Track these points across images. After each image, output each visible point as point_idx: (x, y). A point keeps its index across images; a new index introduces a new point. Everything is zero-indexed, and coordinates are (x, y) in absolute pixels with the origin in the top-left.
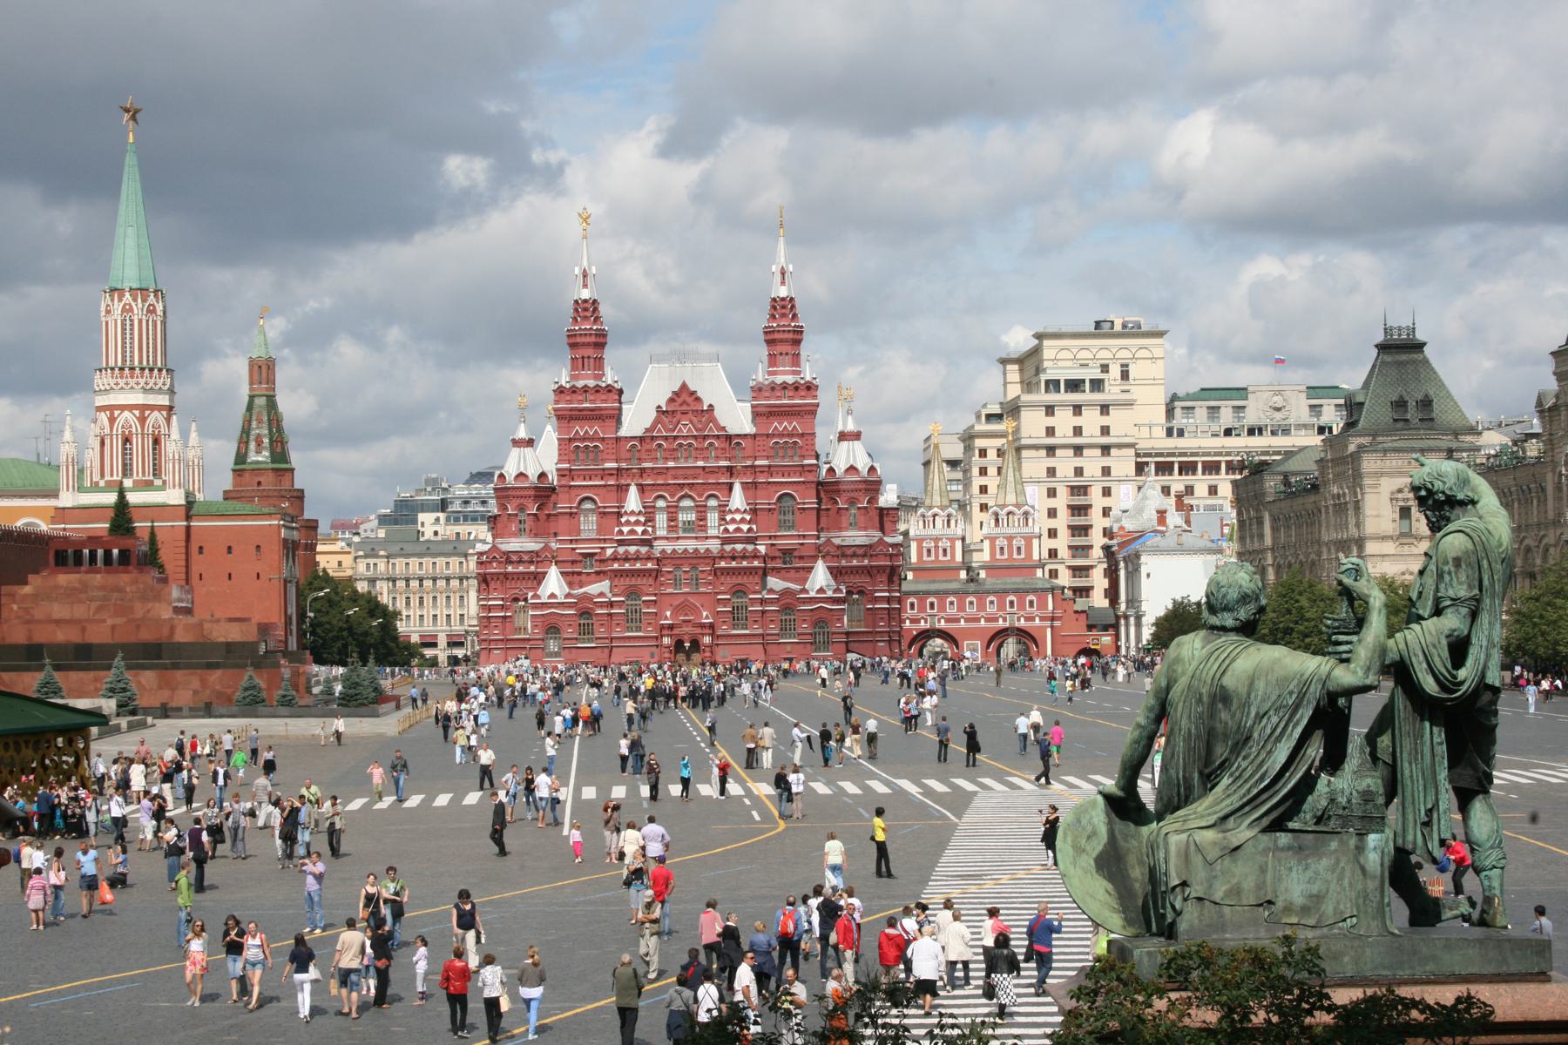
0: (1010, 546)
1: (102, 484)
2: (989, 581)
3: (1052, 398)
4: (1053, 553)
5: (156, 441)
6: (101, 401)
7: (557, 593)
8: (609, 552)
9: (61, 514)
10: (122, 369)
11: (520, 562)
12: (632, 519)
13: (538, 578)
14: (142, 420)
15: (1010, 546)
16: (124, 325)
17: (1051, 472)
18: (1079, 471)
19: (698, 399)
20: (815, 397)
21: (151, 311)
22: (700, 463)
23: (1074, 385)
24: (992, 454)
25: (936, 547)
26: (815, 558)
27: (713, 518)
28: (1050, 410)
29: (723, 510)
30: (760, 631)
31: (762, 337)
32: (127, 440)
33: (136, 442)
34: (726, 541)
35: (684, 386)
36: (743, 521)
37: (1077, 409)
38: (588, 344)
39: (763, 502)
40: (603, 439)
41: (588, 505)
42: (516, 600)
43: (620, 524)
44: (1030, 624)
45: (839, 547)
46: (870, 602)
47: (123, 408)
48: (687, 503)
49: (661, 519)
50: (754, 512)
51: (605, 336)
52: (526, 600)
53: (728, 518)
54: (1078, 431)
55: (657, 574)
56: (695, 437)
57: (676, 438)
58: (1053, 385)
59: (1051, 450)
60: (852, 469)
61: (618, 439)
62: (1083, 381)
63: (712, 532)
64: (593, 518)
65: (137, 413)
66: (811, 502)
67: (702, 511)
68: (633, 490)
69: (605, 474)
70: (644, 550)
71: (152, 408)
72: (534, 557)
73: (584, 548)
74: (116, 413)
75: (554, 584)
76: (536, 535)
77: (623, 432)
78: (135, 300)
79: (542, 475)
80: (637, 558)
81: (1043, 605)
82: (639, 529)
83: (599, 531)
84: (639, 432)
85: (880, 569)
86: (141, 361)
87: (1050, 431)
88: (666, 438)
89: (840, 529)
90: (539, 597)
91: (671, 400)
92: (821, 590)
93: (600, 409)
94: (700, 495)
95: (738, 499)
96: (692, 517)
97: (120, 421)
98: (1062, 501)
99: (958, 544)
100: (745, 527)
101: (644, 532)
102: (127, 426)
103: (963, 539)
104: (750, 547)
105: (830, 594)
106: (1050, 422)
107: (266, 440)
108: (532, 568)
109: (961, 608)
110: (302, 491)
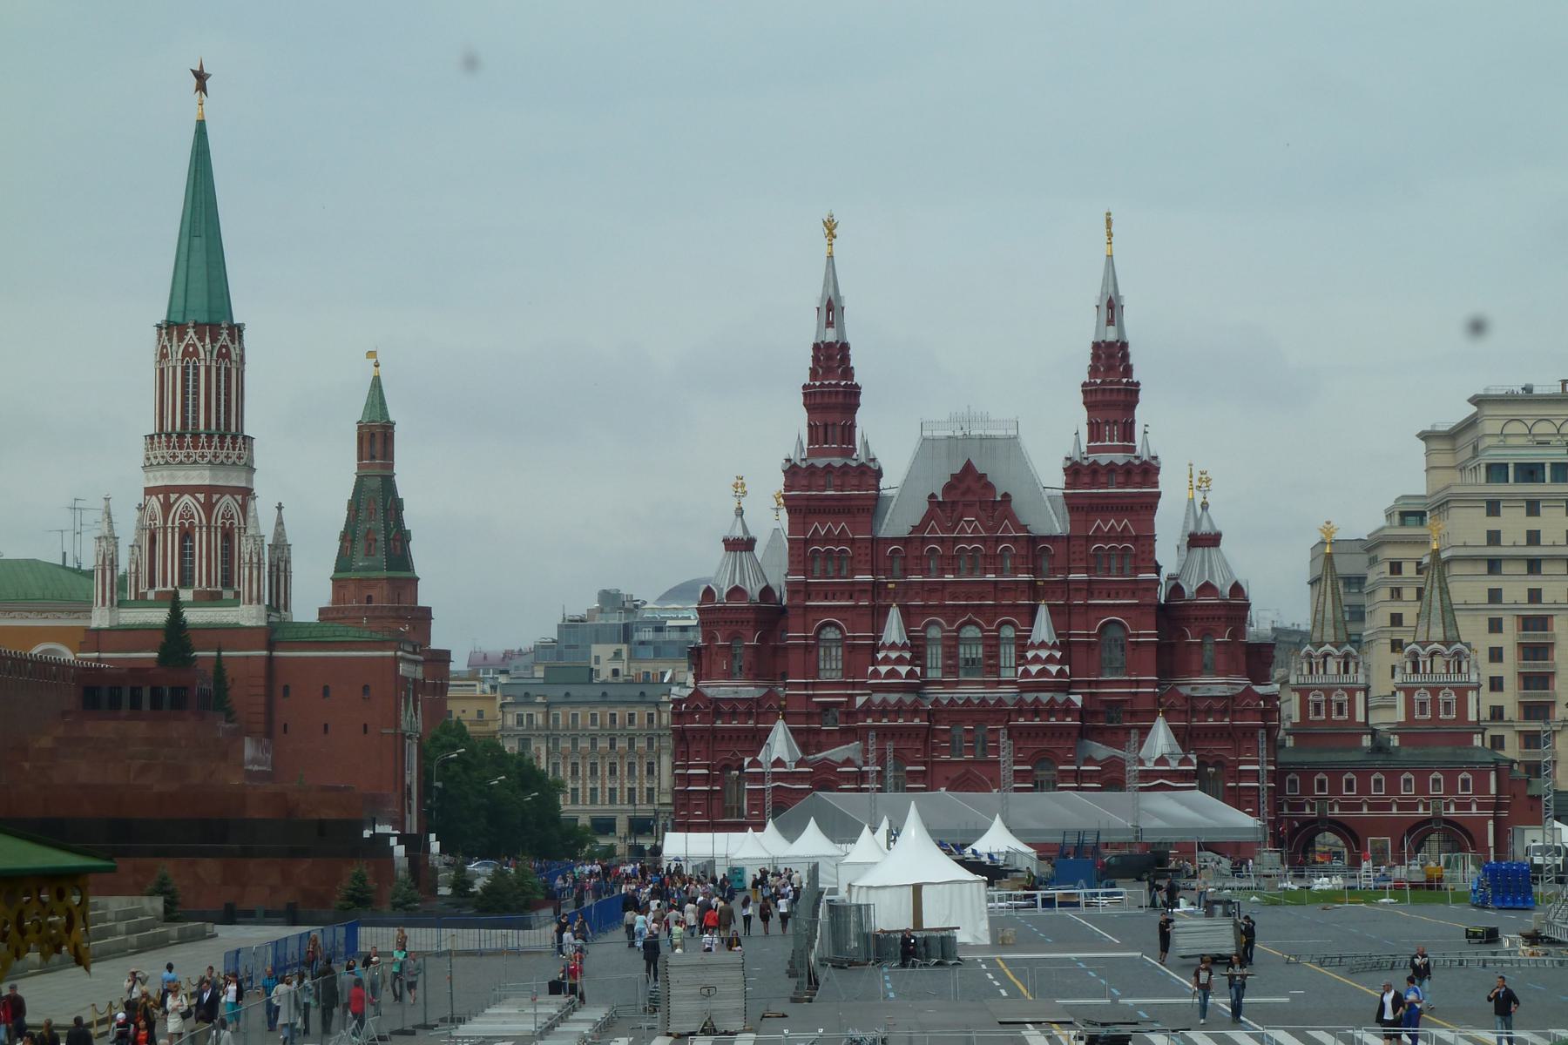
0: (1435, 701)
1: (151, 595)
2: (1404, 751)
3: (1497, 489)
4: (1497, 713)
5: (228, 536)
7: (786, 758)
8: (860, 701)
9: (95, 638)
10: (181, 436)
12: (894, 655)
14: (208, 507)
15: (1435, 701)
17: (1495, 596)
18: (1534, 595)
19: (989, 487)
20: (1156, 485)
21: (224, 355)
22: (991, 577)
23: (1530, 472)
24: (1409, 570)
25: (1329, 702)
26: (1153, 716)
27: (1008, 654)
28: (1493, 508)
29: (1022, 644)
31: (1081, 397)
32: (186, 535)
33: (199, 539)
34: (1025, 688)
35: (969, 467)
36: (1050, 660)
37: (1533, 508)
39: (1079, 634)
40: (852, 542)
41: (831, 634)
42: (727, 768)
43: (874, 662)
44: (1463, 813)
45: (1188, 698)
46: (1232, 778)
47: (182, 490)
48: (971, 632)
49: (935, 655)
50: (1066, 646)
51: (857, 394)
52: (741, 768)
53: (1030, 655)
54: (1533, 538)
55: (929, 732)
56: (983, 540)
57: (956, 540)
58: (1497, 471)
59: (1494, 565)
60: (1207, 588)
61: (876, 543)
62: (1543, 465)
63: (1007, 674)
64: (837, 652)
65: (201, 497)
66: (1149, 635)
67: (992, 645)
68: (894, 616)
69: (852, 590)
70: (909, 699)
71: (222, 490)
72: (753, 708)
73: (823, 696)
74: (173, 497)
75: (780, 745)
76: (757, 676)
78: (201, 339)
79: (767, 592)
80: (899, 709)
81: (1482, 787)
82: (903, 670)
83: (846, 671)
84: (904, 531)
86: (208, 425)
87: (1494, 538)
88: (941, 541)
89: (1190, 674)
90: (759, 765)
91: (948, 488)
92: (1162, 760)
93: (849, 497)
94: (990, 623)
95: (1043, 629)
96: (978, 652)
97: (178, 508)
98: (1508, 639)
99: (1360, 697)
100: (1054, 669)
101: (910, 674)
102: (187, 514)
103: (1367, 690)
104: (1060, 698)
105: (1174, 765)
106: (1493, 523)
107: (381, 537)
108: (751, 724)
109: (1364, 789)
110: (428, 610)
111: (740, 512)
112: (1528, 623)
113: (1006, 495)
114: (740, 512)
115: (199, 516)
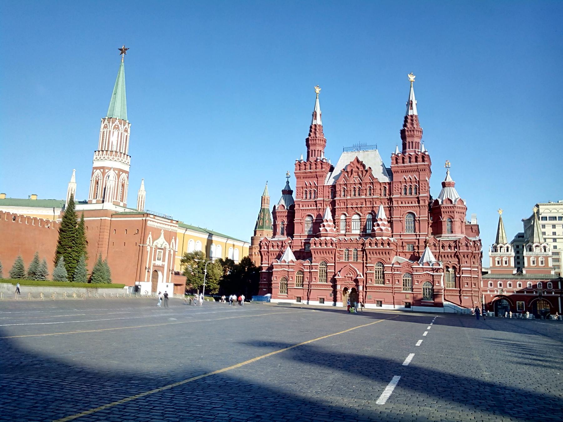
14: (104, 174)
16: (103, 132)
19: (364, 166)
22: (363, 197)
30: (390, 285)
37: (554, 226)
54: (554, 233)
58: (545, 218)
65: (102, 170)
71: (110, 169)
85: (466, 255)
92: (428, 264)
97: (95, 174)
111: (288, 182)
112: (554, 253)
113: (370, 168)
114: (288, 182)
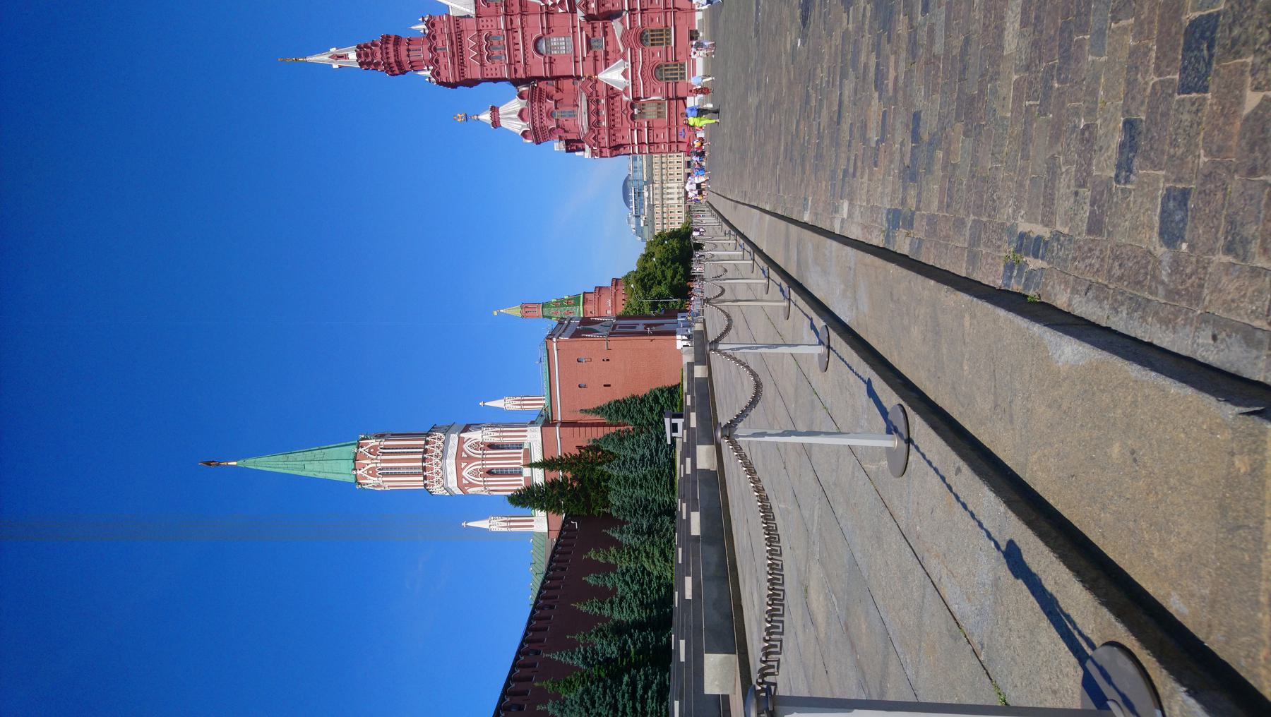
6: (458, 492)
11: (598, 113)
13: (612, 94)
14: (470, 459)
32: (490, 473)
38: (396, 51)
47: (459, 477)
65: (463, 465)
71: (460, 449)
77: (472, 12)
102: (475, 473)
115: (476, 465)
